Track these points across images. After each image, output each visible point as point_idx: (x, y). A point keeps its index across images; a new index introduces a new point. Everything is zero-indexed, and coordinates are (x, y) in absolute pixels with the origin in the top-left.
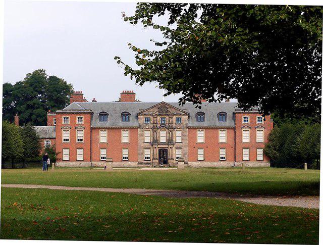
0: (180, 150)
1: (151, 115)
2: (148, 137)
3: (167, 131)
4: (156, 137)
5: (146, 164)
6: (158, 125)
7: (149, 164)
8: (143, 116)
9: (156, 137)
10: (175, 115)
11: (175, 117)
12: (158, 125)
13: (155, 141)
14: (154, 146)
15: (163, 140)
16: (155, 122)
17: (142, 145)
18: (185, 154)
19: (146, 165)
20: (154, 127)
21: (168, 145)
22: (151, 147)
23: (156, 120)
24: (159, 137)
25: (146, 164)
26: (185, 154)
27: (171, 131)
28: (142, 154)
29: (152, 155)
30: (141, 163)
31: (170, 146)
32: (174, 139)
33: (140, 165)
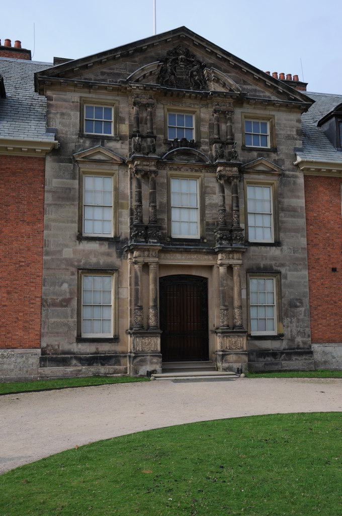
0: (270, 285)
1: (122, 90)
2: (104, 206)
5: (91, 360)
7: (104, 359)
8: (75, 96)
10: (241, 100)
11: (238, 113)
17: (68, 253)
18: (292, 305)
19: (93, 369)
20: (138, 148)
22: (114, 260)
24: (167, 208)
25: (91, 360)
26: (292, 305)
27: (228, 180)
28: (66, 303)
30: (62, 359)
33: (52, 371)
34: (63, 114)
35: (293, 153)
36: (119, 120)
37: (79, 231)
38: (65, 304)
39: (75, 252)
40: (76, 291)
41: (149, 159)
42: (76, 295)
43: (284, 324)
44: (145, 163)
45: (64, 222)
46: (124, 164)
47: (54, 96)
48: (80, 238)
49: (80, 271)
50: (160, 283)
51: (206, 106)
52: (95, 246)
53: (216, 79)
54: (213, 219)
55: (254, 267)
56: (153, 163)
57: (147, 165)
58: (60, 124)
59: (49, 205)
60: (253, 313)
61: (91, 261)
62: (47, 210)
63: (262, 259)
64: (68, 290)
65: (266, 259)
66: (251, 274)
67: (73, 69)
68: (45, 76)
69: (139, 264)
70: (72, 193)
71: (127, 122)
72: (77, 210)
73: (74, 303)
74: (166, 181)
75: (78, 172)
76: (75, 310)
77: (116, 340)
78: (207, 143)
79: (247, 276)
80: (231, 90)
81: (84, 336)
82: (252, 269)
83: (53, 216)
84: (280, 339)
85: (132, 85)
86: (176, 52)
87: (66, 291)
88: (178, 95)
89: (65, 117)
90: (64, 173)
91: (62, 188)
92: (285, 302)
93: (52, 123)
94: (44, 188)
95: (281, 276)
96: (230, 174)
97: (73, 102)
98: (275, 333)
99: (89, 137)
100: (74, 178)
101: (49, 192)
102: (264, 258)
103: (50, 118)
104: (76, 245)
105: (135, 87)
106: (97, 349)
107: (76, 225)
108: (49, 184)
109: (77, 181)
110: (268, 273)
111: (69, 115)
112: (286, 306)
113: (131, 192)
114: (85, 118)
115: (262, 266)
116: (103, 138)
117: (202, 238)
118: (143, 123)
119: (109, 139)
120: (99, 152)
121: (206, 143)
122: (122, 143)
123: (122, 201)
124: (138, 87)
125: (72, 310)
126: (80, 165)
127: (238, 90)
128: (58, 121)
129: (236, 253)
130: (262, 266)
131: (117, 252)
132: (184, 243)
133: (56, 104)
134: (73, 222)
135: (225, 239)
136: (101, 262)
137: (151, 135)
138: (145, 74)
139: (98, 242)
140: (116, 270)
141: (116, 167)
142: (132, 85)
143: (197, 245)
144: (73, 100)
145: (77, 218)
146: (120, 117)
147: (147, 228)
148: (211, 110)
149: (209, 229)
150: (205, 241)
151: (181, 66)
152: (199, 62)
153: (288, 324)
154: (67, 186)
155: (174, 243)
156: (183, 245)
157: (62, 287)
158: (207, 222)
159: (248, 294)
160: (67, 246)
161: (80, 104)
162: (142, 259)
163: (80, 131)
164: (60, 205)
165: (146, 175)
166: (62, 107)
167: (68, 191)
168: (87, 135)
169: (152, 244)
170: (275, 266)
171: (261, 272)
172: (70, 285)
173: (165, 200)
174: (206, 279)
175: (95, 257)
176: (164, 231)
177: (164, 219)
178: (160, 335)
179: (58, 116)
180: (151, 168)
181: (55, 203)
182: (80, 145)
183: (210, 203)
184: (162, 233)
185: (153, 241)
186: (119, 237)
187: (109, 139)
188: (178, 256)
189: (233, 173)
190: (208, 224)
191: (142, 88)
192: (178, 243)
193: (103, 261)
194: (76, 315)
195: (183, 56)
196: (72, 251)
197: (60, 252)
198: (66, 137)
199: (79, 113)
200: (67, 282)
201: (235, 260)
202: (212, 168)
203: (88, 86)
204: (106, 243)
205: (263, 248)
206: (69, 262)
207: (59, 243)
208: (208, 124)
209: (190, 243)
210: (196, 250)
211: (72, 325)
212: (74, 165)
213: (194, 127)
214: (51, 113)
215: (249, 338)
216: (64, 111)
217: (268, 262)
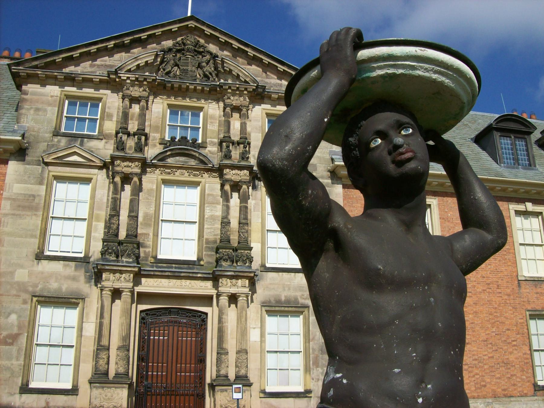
3: (212, 184)
4: (133, 216)
6: (152, 151)
9: (133, 216)
12: (152, 151)
13: (122, 248)
14: (110, 281)
15: (178, 242)
16: (133, 127)
17: (21, 275)
21: (215, 279)
23: (142, 116)
24: (156, 220)
27: (236, 187)
28: (13, 339)
29: (89, 347)
31: (228, 287)
32: (256, 246)
34: (37, 110)
35: (328, 157)
36: (106, 116)
37: (39, 248)
38: (11, 341)
39: (30, 274)
40: (27, 324)
41: (132, 160)
42: (26, 330)
43: (313, 376)
44: (126, 164)
45: (21, 236)
46: (105, 166)
47: (30, 90)
48: (40, 256)
49: (35, 299)
50: (142, 319)
51: (218, 101)
52: (58, 266)
53: (228, 70)
54: (215, 235)
55: (272, 300)
56: (137, 163)
57: (128, 166)
58: (32, 120)
59: (6, 215)
60: (271, 360)
61: (49, 286)
62: (2, 221)
63: (284, 290)
64: (16, 323)
65: (289, 289)
66: (268, 308)
67: (55, 60)
68: (21, 68)
69: (107, 289)
70: (37, 200)
71: (115, 119)
72: (40, 222)
73: (23, 340)
74: (155, 187)
75: (47, 176)
76: (22, 350)
77: (74, 391)
78: (216, 144)
79: (261, 310)
80: (246, 82)
81: (33, 385)
82: (270, 302)
83: (7, 229)
84: (306, 397)
85: (121, 75)
86: (183, 42)
87: (13, 325)
88: (180, 87)
89: (40, 113)
90: (29, 177)
91: (24, 194)
92: (315, 347)
93: (22, 120)
94: (2, 194)
95: (309, 312)
96: (237, 178)
97: (52, 96)
98: (301, 389)
99: (65, 135)
100: (41, 183)
101: (8, 199)
102: (286, 289)
103: (21, 114)
104: (33, 265)
105: (125, 78)
106: (47, 403)
107: (37, 241)
108: (9, 190)
109: (44, 187)
110: (292, 307)
111: (45, 111)
112: (316, 353)
113: (108, 199)
114: (65, 114)
115: (283, 299)
116: (83, 137)
117: (199, 259)
118: (134, 119)
119: (90, 137)
120: (75, 153)
121: (213, 144)
122: (106, 143)
123: (99, 212)
124: (128, 78)
125: (19, 350)
126: (51, 168)
127: (255, 81)
128: (30, 117)
129: (241, 279)
130: (283, 299)
131: (85, 275)
132: (174, 265)
133: (31, 99)
134: (33, 236)
135: (226, 260)
136: (64, 288)
137: (141, 133)
138: (139, 64)
139: (62, 262)
140: (82, 299)
141: (96, 171)
142: (121, 75)
143: (190, 269)
144: (52, 94)
145: (38, 232)
146: (107, 113)
147: (120, 243)
148: (221, 104)
149: (209, 247)
150: (202, 263)
151: (188, 56)
152: (211, 54)
153: (318, 376)
154: (30, 193)
155: (160, 265)
156: (172, 267)
157: (9, 318)
158: (207, 239)
159: (262, 335)
160: (22, 267)
161: (60, 98)
162: (111, 284)
163: (55, 129)
164: (20, 215)
165: (126, 179)
166: (37, 102)
167: (32, 198)
168: (64, 133)
169: (124, 264)
170: (301, 297)
171: (282, 306)
172: (19, 316)
173: (152, 210)
174: (206, 314)
175: (56, 281)
176: (147, 250)
177: (149, 235)
178: (127, 386)
179: (32, 112)
180: (133, 170)
181: (13, 212)
182: (53, 146)
183: (212, 216)
184: (145, 252)
185: (127, 260)
186: (90, 258)
187: (90, 137)
188: (164, 282)
189: (242, 177)
190: (208, 242)
191: (134, 79)
192: (165, 265)
193: (65, 287)
194: (23, 356)
195: (189, 46)
196: (29, 273)
197: (12, 273)
198: (38, 135)
199: (57, 109)
200: (16, 313)
201: (240, 287)
202: (219, 171)
203: (71, 79)
204: (73, 264)
205: (285, 275)
206: (22, 287)
207: (12, 262)
208: (218, 122)
209: (182, 266)
210: (188, 274)
211: (18, 369)
212: (43, 168)
213: (201, 125)
214: (23, 109)
215: (262, 395)
216: (40, 106)
217: (291, 294)
